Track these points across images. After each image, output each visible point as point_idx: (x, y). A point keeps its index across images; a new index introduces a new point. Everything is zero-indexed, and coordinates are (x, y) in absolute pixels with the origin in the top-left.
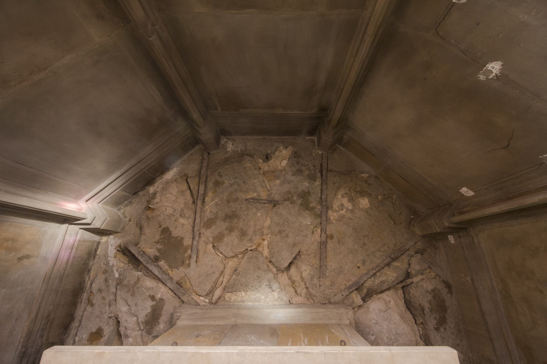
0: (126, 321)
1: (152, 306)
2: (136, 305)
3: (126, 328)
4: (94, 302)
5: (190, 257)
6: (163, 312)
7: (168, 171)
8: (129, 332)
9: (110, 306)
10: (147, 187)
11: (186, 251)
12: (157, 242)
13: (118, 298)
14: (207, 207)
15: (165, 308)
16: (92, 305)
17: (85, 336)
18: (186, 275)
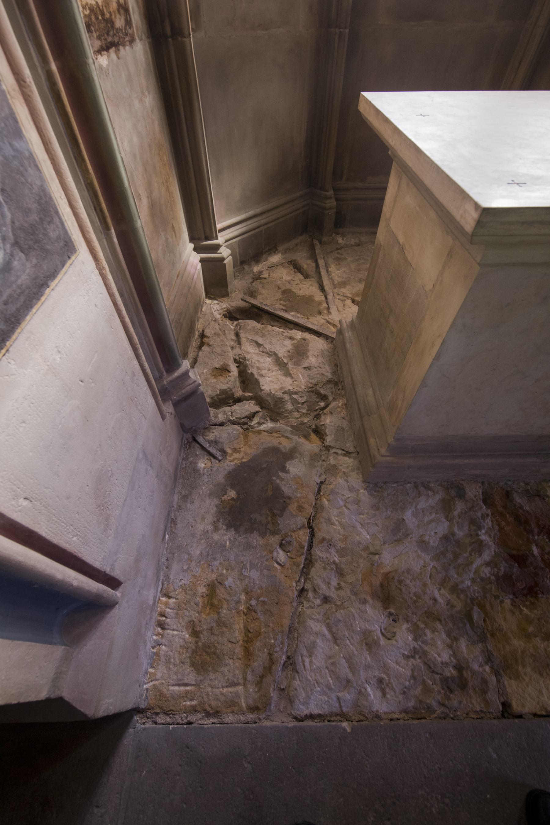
0: (258, 361)
1: (292, 345)
2: (271, 343)
3: (258, 368)
4: (211, 343)
5: (328, 308)
6: (310, 348)
7: (275, 252)
8: (263, 372)
9: (232, 348)
10: (253, 263)
11: (320, 303)
12: (281, 300)
13: (243, 340)
14: (333, 275)
15: (311, 345)
16: (209, 345)
17: (205, 371)
18: (328, 322)
